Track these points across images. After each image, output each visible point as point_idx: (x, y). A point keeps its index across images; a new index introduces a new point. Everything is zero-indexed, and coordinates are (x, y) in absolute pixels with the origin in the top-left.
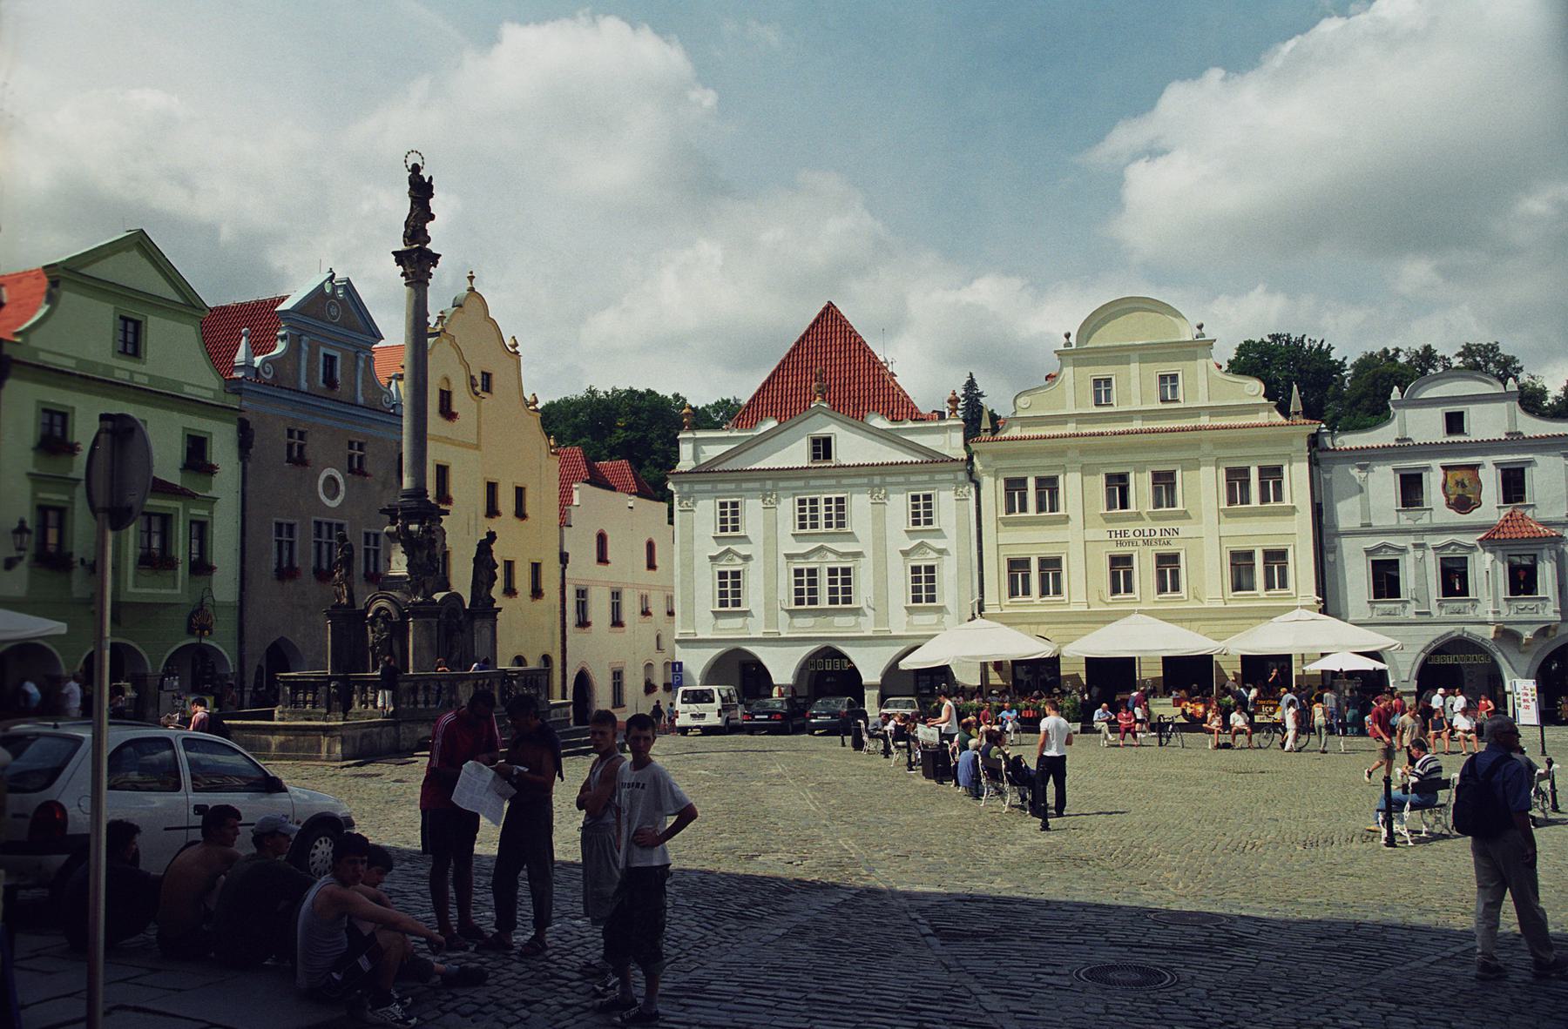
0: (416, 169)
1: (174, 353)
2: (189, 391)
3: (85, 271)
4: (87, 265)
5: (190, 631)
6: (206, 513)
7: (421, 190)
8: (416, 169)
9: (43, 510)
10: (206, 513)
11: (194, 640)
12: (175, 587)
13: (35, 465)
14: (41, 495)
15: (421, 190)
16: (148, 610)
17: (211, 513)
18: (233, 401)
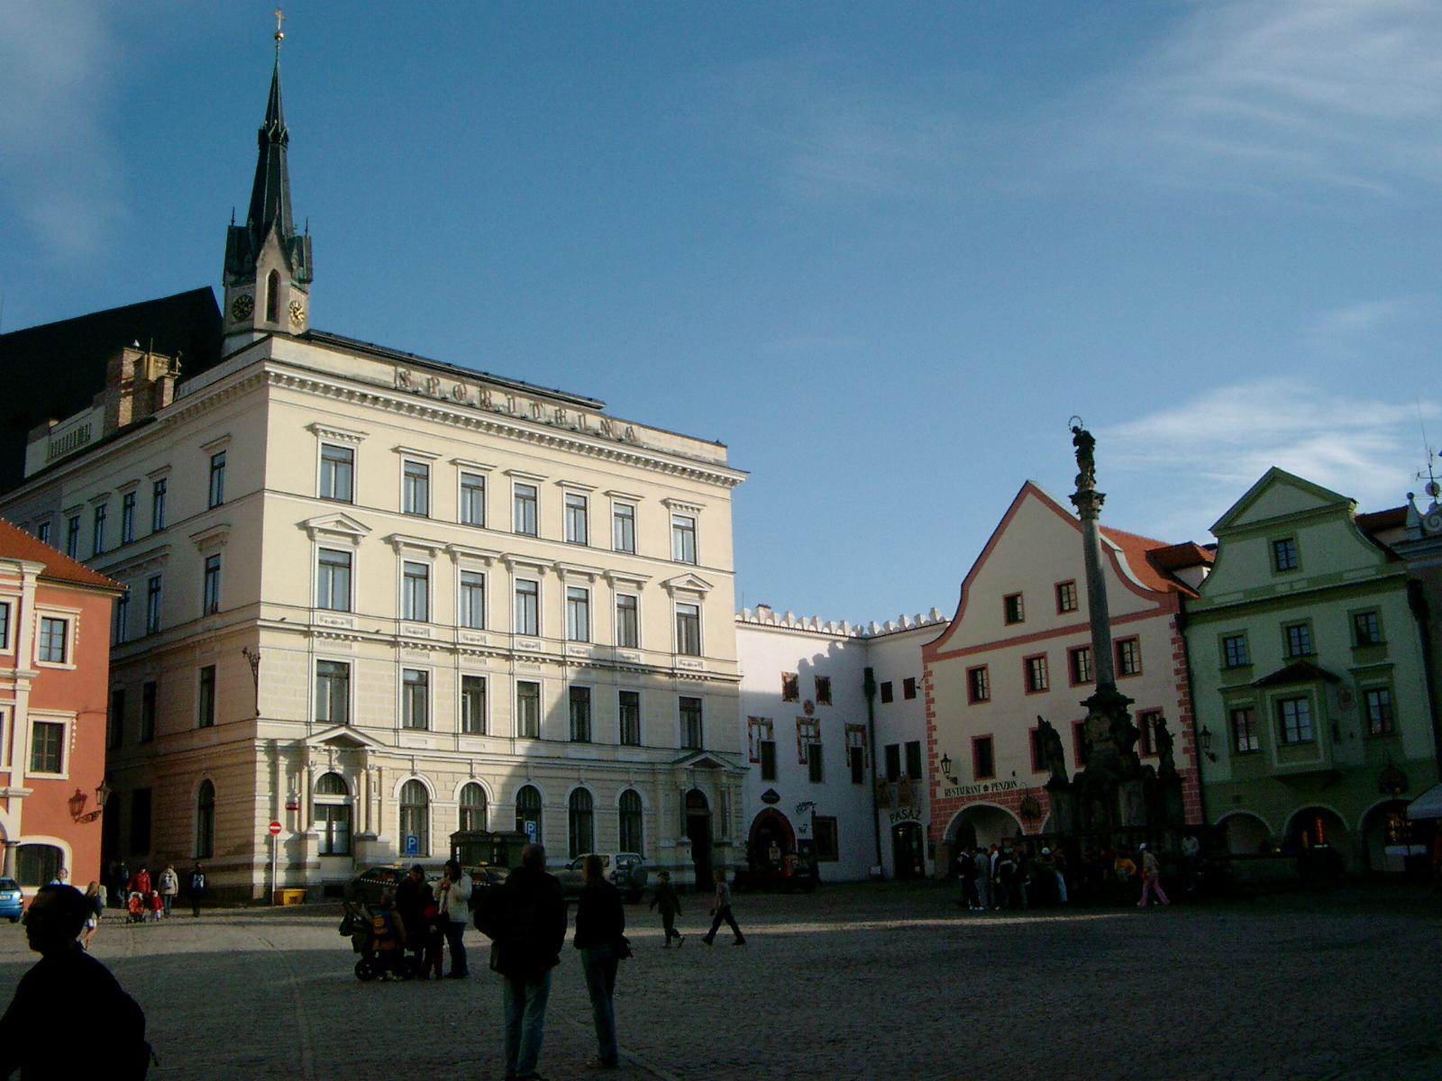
0: (1075, 430)
1: (1328, 553)
2: (1350, 578)
3: (1239, 522)
4: (1237, 517)
5: (1382, 791)
6: (1385, 679)
7: (1084, 443)
8: (1075, 430)
9: (1233, 714)
10: (1385, 679)
11: (1389, 798)
12: (1317, 757)
13: (1224, 681)
14: (1230, 703)
15: (1084, 443)
16: (1332, 778)
17: (1391, 677)
18: (1398, 569)
